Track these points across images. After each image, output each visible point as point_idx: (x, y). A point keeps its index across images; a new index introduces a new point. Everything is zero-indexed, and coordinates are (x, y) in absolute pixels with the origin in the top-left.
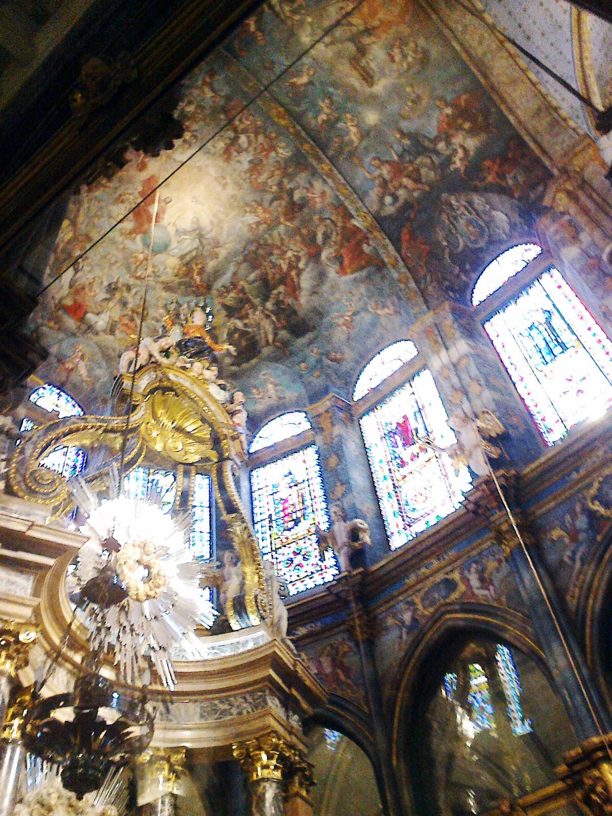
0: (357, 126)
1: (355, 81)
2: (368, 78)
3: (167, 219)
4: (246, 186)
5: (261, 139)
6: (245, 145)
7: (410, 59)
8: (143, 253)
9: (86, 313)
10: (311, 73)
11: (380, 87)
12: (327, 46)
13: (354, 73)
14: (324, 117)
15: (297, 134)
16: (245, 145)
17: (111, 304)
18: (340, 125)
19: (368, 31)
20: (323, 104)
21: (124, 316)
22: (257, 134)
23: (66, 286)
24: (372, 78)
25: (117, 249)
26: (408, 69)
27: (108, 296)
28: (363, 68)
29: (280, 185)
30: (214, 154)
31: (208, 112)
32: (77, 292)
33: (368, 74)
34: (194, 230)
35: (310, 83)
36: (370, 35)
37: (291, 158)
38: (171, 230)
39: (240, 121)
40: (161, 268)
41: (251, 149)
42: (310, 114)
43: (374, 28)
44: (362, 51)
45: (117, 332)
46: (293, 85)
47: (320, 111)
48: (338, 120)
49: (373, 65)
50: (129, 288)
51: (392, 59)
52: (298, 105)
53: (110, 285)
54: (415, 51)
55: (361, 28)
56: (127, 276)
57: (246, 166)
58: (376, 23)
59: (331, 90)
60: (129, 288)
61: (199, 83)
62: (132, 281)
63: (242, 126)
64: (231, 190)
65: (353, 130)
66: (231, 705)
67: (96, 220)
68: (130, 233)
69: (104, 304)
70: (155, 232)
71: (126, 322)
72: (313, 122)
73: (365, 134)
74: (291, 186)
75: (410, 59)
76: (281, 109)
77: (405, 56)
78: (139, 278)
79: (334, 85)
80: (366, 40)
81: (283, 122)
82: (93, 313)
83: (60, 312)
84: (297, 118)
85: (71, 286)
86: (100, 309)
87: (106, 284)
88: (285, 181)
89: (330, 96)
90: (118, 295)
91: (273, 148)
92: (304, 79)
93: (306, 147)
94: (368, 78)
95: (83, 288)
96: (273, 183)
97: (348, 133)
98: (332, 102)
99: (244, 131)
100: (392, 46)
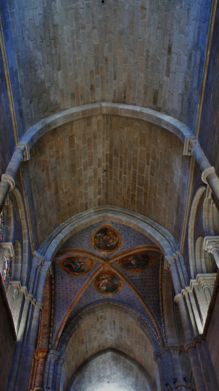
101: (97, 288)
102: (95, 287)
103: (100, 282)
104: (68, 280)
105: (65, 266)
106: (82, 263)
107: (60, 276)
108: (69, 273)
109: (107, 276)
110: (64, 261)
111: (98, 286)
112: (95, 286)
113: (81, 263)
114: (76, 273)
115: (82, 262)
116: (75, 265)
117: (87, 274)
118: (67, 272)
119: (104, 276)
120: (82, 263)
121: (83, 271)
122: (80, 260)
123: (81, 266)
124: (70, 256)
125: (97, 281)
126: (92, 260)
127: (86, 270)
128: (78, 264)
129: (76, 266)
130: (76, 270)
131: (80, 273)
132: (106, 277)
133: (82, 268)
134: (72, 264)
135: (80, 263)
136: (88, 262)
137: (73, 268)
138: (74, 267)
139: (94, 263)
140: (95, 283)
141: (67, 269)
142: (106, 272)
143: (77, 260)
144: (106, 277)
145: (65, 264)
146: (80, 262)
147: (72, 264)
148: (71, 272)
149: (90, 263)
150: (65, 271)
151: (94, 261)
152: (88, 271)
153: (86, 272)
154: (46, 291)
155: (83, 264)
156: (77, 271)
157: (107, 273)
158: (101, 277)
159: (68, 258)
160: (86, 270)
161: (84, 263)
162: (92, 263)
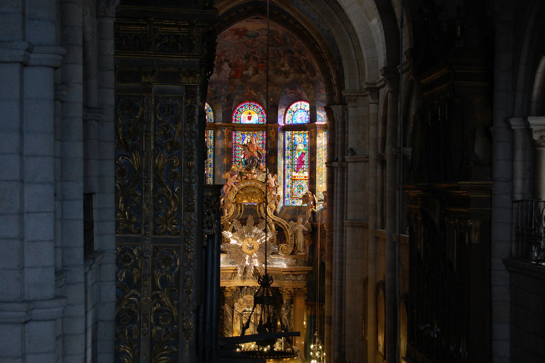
8: (250, 40)
9: (242, 73)
17: (251, 63)
21: (258, 63)
27: (247, 60)
40: (262, 40)
45: (259, 72)
50: (254, 53)
53: (245, 56)
56: (250, 49)
60: (254, 53)
62: (253, 50)
66: (280, 276)
71: (261, 65)
78: (256, 47)
83: (232, 80)
87: (243, 57)
90: (251, 58)
95: (236, 64)
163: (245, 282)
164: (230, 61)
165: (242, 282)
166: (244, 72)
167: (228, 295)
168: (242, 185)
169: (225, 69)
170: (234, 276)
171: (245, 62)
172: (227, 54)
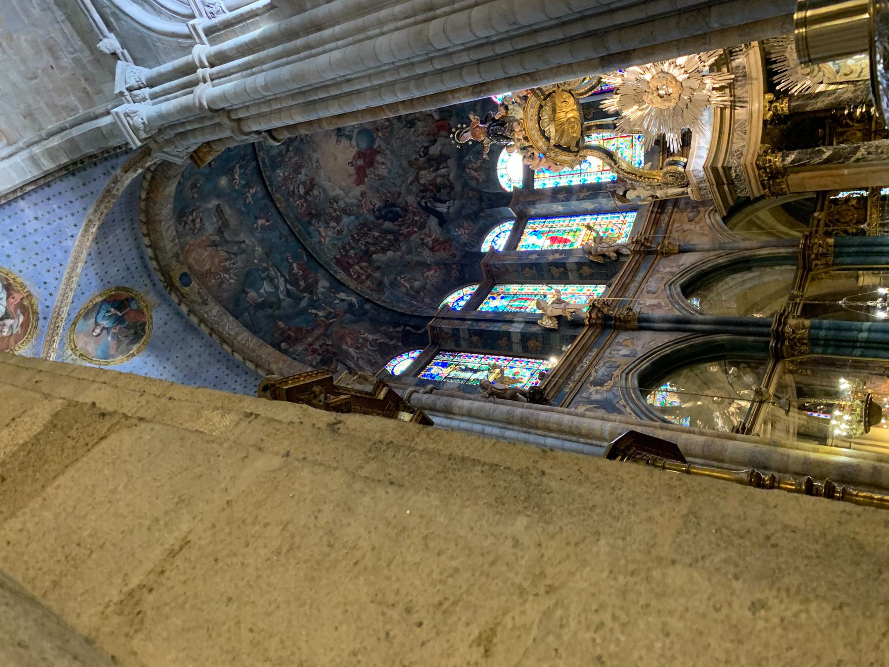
0: (234, 179)
1: (227, 211)
2: (219, 210)
3: (353, 152)
4: (306, 156)
5: (291, 189)
6: (301, 187)
7: (191, 218)
9: (438, 121)
10: (255, 226)
11: (214, 202)
12: (244, 242)
13: (227, 217)
14: (251, 191)
15: (271, 184)
16: (301, 187)
18: (243, 182)
19: (215, 244)
20: (250, 199)
22: (293, 191)
23: (438, 143)
24: (217, 210)
25: (392, 146)
26: (193, 211)
27: (416, 121)
28: (221, 219)
29: (288, 151)
30: (320, 187)
31: (322, 218)
32: (434, 135)
33: (219, 214)
34: (341, 136)
35: (257, 218)
36: (214, 242)
37: (277, 168)
38: (354, 143)
39: (302, 206)
41: (298, 182)
42: (260, 195)
43: (211, 246)
44: (220, 231)
46: (268, 221)
47: (253, 196)
48: (244, 187)
49: (215, 220)
51: (201, 219)
52: (266, 205)
53: (410, 127)
54: (186, 223)
55: (219, 248)
56: (396, 126)
57: (303, 171)
58: (209, 249)
59: (244, 209)
61: (328, 239)
63: (302, 201)
64: (315, 156)
65: (237, 176)
67: (401, 172)
68: (379, 152)
69: (422, 118)
70: (364, 145)
72: (259, 189)
73: (231, 171)
74: (283, 147)
75: (191, 218)
76: (278, 205)
77: (193, 221)
79: (242, 213)
80: (216, 238)
81: (278, 196)
82: (433, 118)
84: (269, 195)
85: (436, 141)
86: (427, 117)
87: (413, 130)
88: (284, 152)
89: (245, 205)
91: (285, 179)
92: (261, 222)
93: (268, 174)
94: (219, 210)
95: (428, 135)
96: (291, 154)
97: (240, 174)
98: (245, 200)
99: (300, 197)
100: (200, 229)
101: (7, 280)
102: (19, 280)
103: (11, 300)
104: (113, 271)
105: (133, 299)
106: (98, 331)
107: (133, 268)
108: (117, 289)
109: (5, 334)
110: (140, 311)
111: (10, 284)
112: (22, 285)
113: (102, 331)
114: (100, 299)
115: (98, 336)
116: (110, 316)
117: (73, 316)
118: (124, 289)
119: (11, 327)
120: (98, 331)
121: (86, 315)
122: (110, 338)
123: (97, 324)
124: (143, 340)
125: (26, 303)
126: (81, 355)
127: (81, 321)
128: (105, 323)
129: (107, 314)
130: (103, 306)
131: (90, 307)
132: (4, 325)
133: (93, 320)
134: (120, 314)
135: (104, 328)
136: (86, 343)
137: (112, 307)
138: (112, 310)
139: (70, 352)
140: (29, 296)
141: (125, 295)
142: (16, 343)
143: (114, 333)
144: (4, 325)
145: (134, 306)
146: (105, 332)
147: (120, 314)
148: (113, 293)
149: (80, 344)
150: (127, 288)
151: (74, 357)
152: (74, 324)
153: (77, 318)
154: (169, 232)
155: (93, 331)
156: (100, 307)
157: (12, 340)
158: (21, 319)
159: (144, 331)
160: (81, 321)
161: (95, 334)
162: (74, 349)
163: (754, 75)
164: (426, 145)
165: (754, 82)
166: (436, 118)
167: (783, 106)
168: (541, 143)
169: (439, 148)
170: (740, 102)
171: (419, 124)
172: (414, 157)
